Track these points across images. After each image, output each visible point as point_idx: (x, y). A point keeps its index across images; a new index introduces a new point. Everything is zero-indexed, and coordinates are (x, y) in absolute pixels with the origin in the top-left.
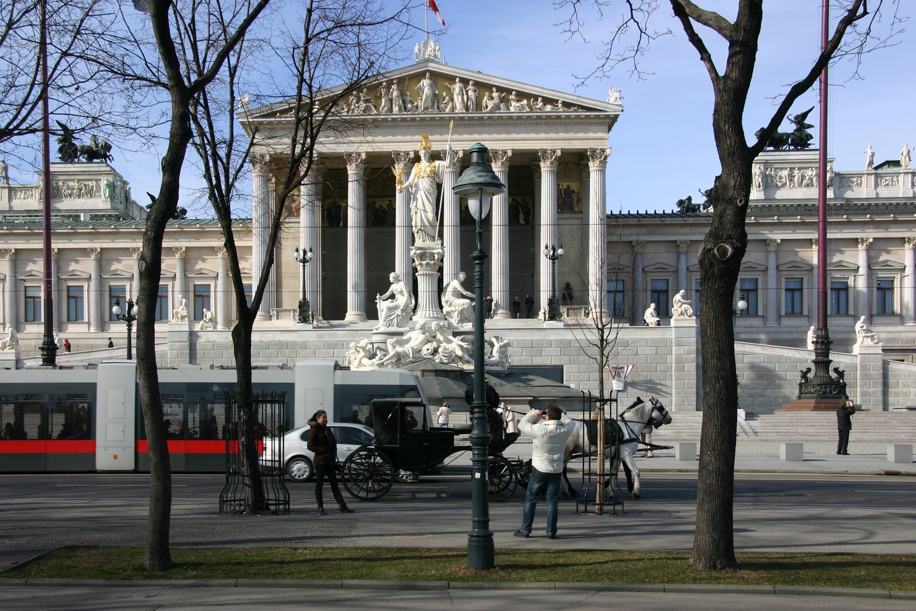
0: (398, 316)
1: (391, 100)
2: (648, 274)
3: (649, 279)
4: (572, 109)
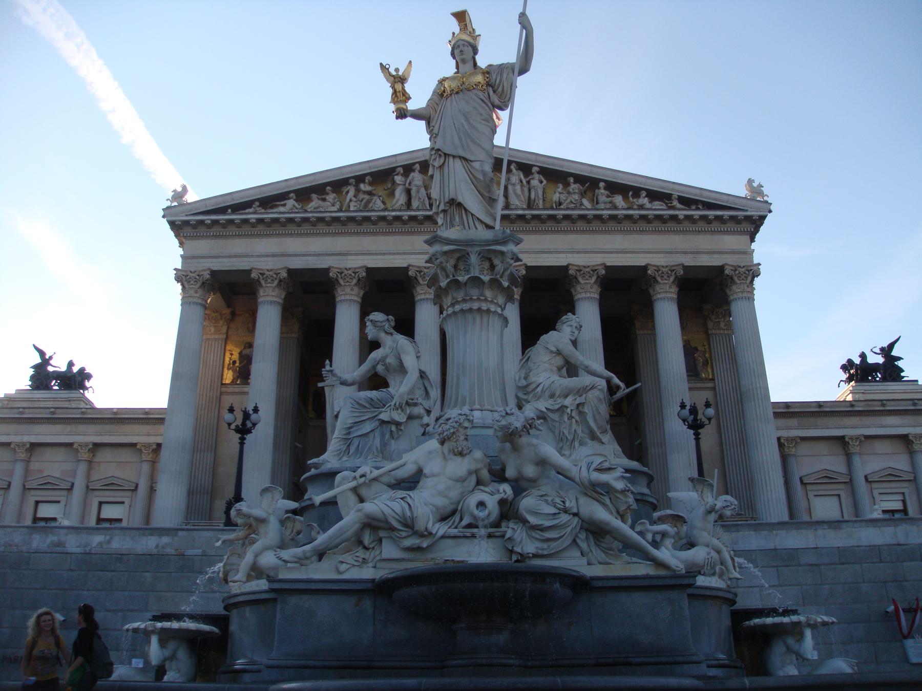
0: (383, 422)
1: (408, 192)
2: (809, 487)
3: (811, 495)
4: (694, 207)
